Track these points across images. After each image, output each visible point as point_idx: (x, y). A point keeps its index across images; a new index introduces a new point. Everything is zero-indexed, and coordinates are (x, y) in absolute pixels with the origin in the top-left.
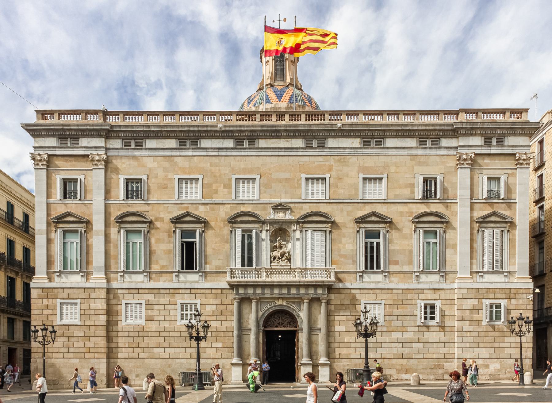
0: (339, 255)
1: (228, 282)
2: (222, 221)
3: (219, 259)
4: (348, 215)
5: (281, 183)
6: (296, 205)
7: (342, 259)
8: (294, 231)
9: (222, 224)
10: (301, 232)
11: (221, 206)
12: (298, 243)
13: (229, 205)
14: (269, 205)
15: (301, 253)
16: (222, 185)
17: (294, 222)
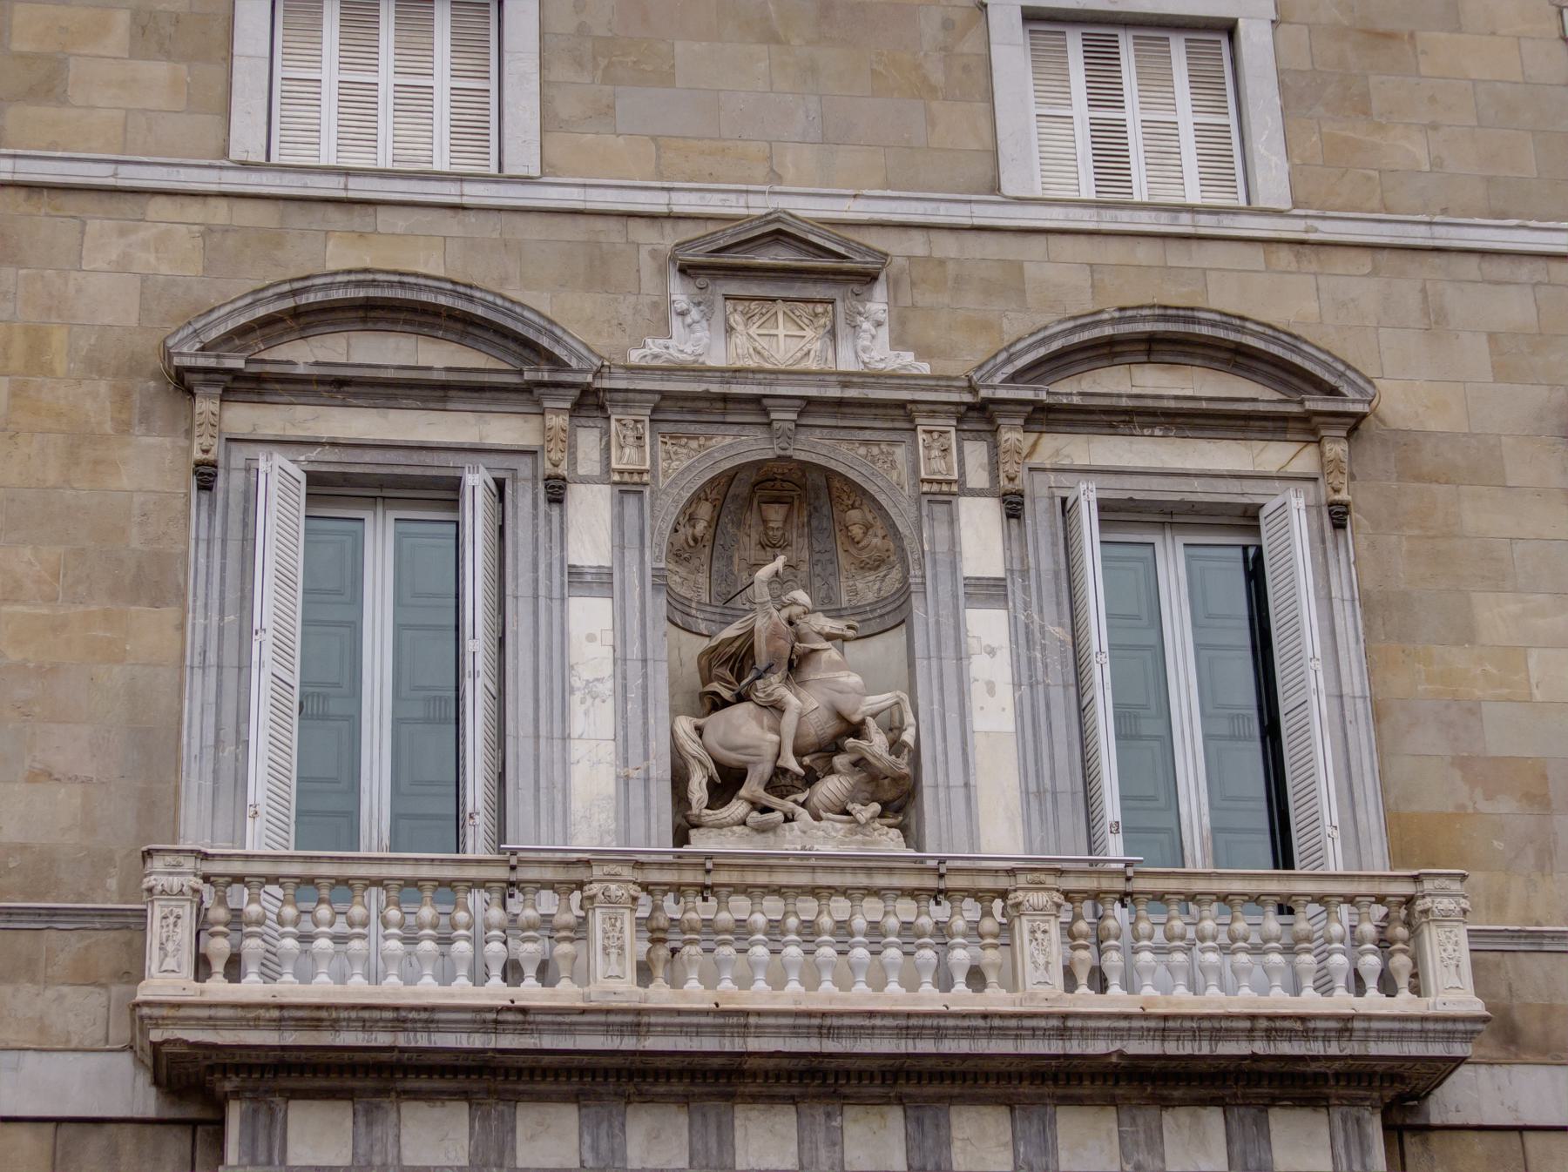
0: (1463, 764)
1: (140, 1014)
2: (95, 366)
3: (46, 775)
4: (1502, 372)
5: (771, 38)
6: (947, 246)
7: (1505, 806)
8: (943, 495)
9: (95, 402)
10: (1014, 507)
11: (100, 224)
12: (988, 627)
13: (195, 212)
14: (644, 234)
15: (1031, 722)
16: (122, 18)
17: (934, 409)
